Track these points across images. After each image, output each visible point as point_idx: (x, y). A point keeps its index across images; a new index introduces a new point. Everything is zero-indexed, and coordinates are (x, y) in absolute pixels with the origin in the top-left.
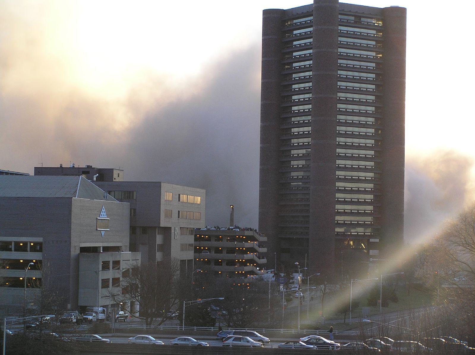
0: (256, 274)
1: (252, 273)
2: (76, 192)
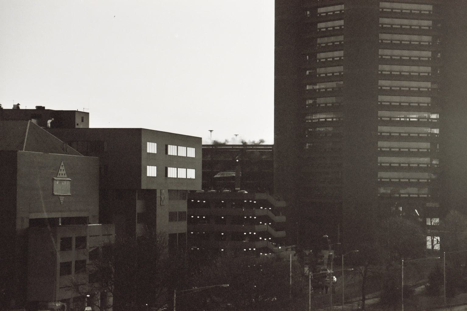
0: (272, 252)
1: (266, 249)
2: (22, 143)
